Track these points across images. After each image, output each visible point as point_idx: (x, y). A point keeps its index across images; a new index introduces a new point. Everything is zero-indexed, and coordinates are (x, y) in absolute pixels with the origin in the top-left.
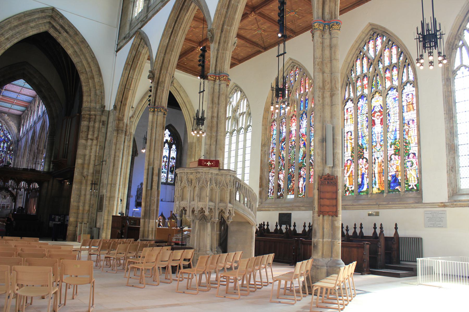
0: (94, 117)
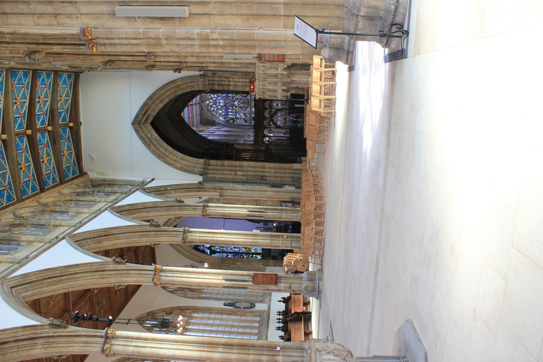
0: (210, 82)
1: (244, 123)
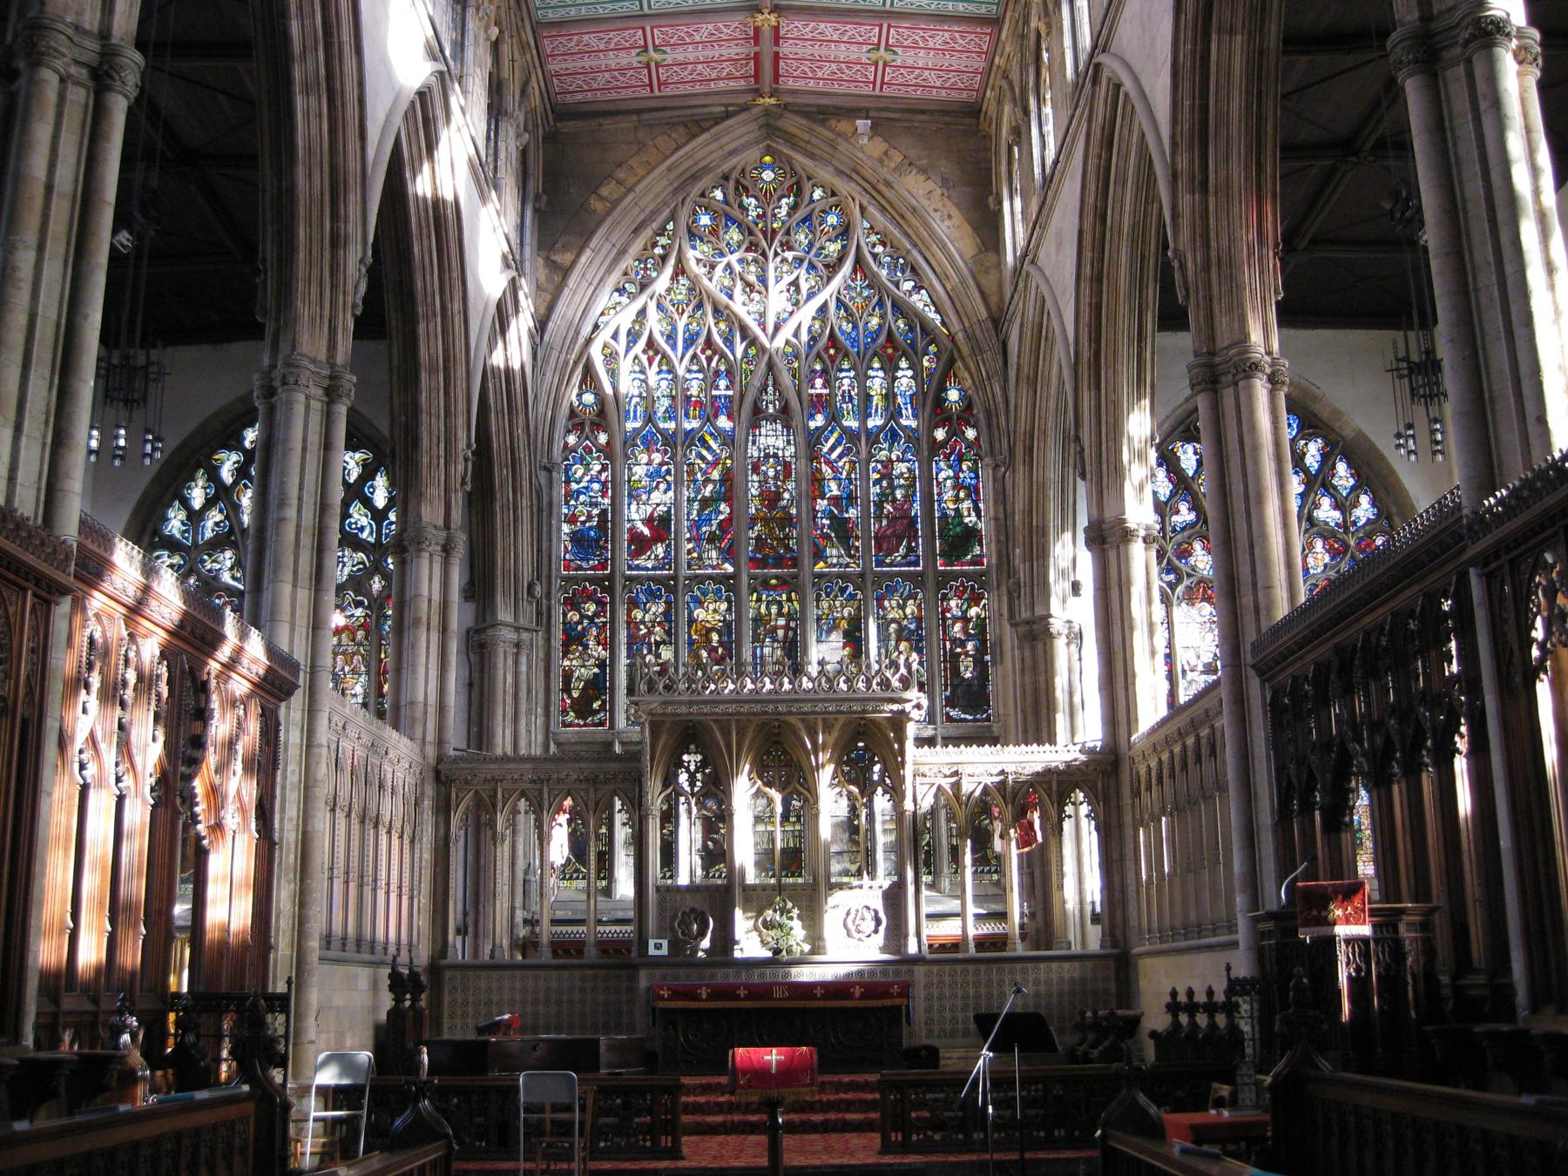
1: (572, 519)
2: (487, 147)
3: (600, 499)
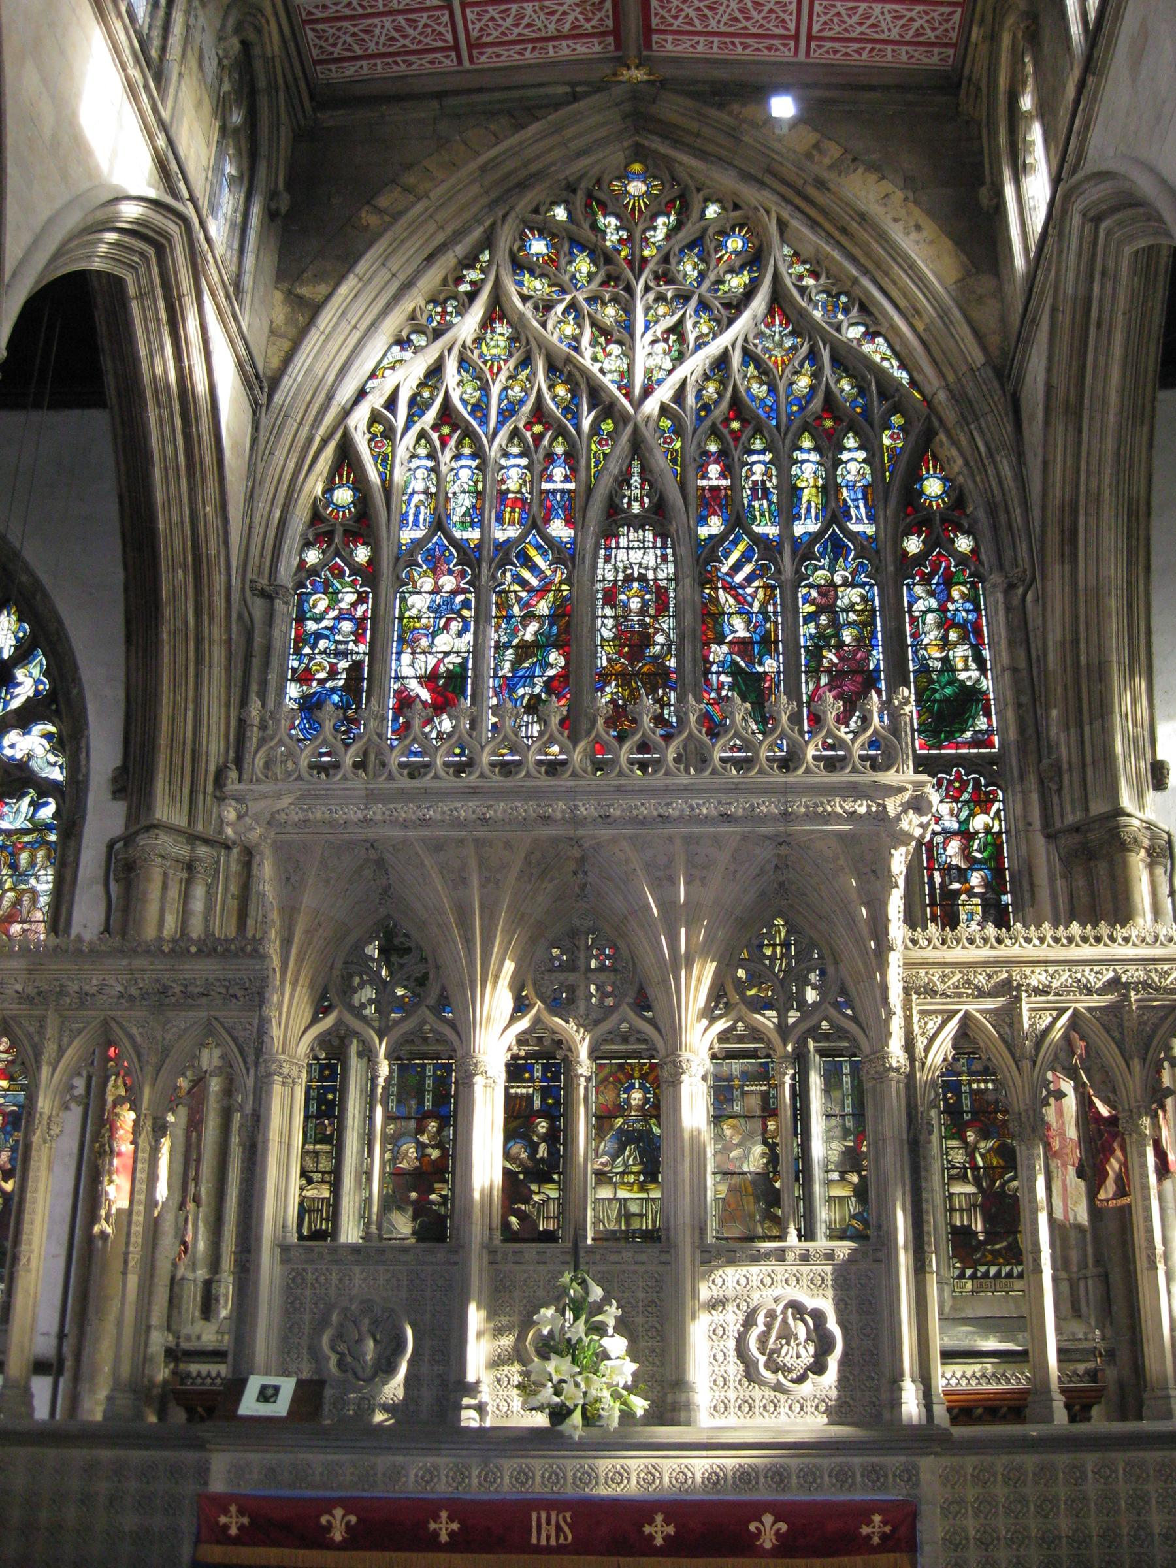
1: (304, 677)
2: (152, 15)
3: (351, 646)
